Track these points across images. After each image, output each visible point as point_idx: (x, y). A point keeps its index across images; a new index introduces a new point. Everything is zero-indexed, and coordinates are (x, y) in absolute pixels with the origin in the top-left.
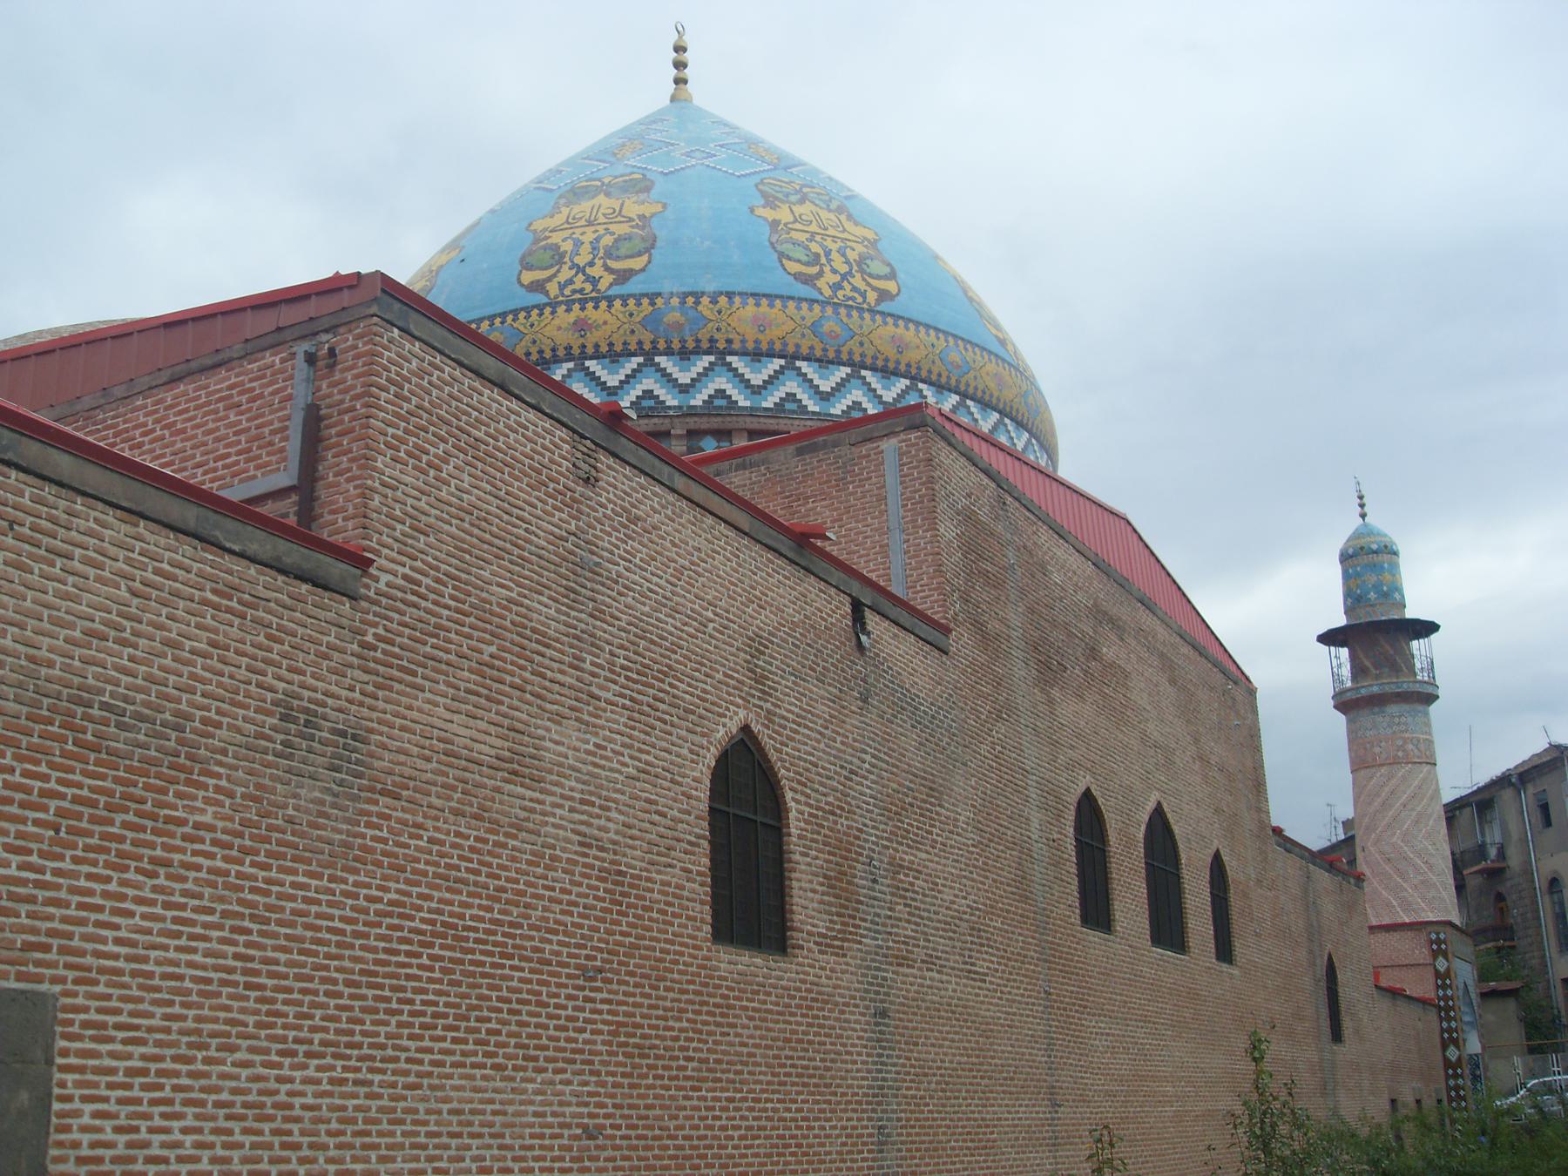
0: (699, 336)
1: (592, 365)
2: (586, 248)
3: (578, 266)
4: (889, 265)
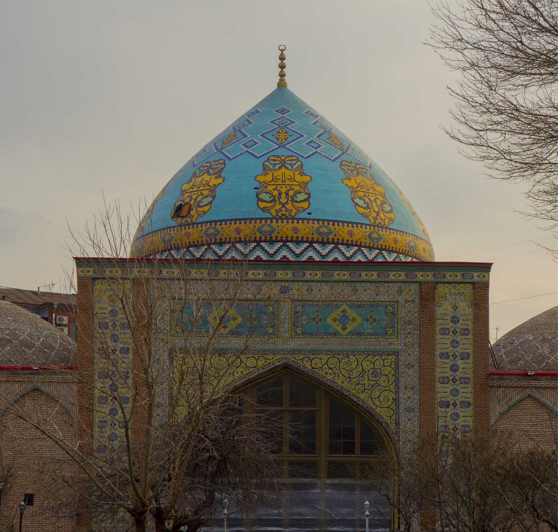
0: (329, 237)
1: (290, 244)
2: (283, 195)
3: (282, 203)
4: (391, 206)
